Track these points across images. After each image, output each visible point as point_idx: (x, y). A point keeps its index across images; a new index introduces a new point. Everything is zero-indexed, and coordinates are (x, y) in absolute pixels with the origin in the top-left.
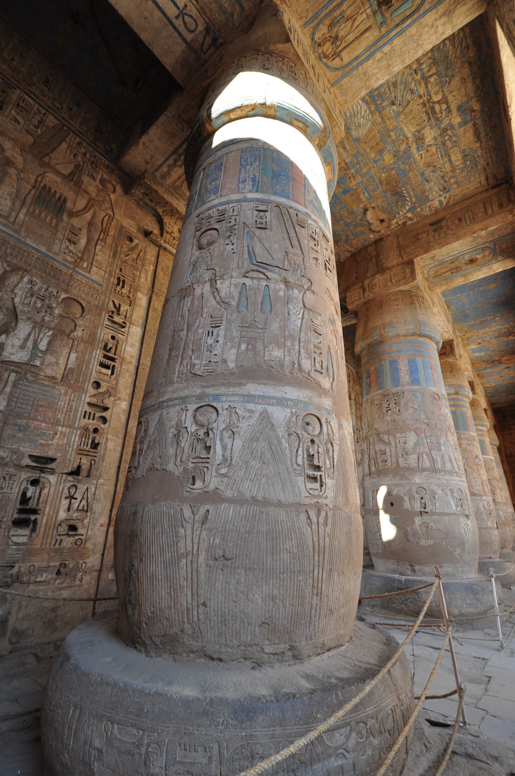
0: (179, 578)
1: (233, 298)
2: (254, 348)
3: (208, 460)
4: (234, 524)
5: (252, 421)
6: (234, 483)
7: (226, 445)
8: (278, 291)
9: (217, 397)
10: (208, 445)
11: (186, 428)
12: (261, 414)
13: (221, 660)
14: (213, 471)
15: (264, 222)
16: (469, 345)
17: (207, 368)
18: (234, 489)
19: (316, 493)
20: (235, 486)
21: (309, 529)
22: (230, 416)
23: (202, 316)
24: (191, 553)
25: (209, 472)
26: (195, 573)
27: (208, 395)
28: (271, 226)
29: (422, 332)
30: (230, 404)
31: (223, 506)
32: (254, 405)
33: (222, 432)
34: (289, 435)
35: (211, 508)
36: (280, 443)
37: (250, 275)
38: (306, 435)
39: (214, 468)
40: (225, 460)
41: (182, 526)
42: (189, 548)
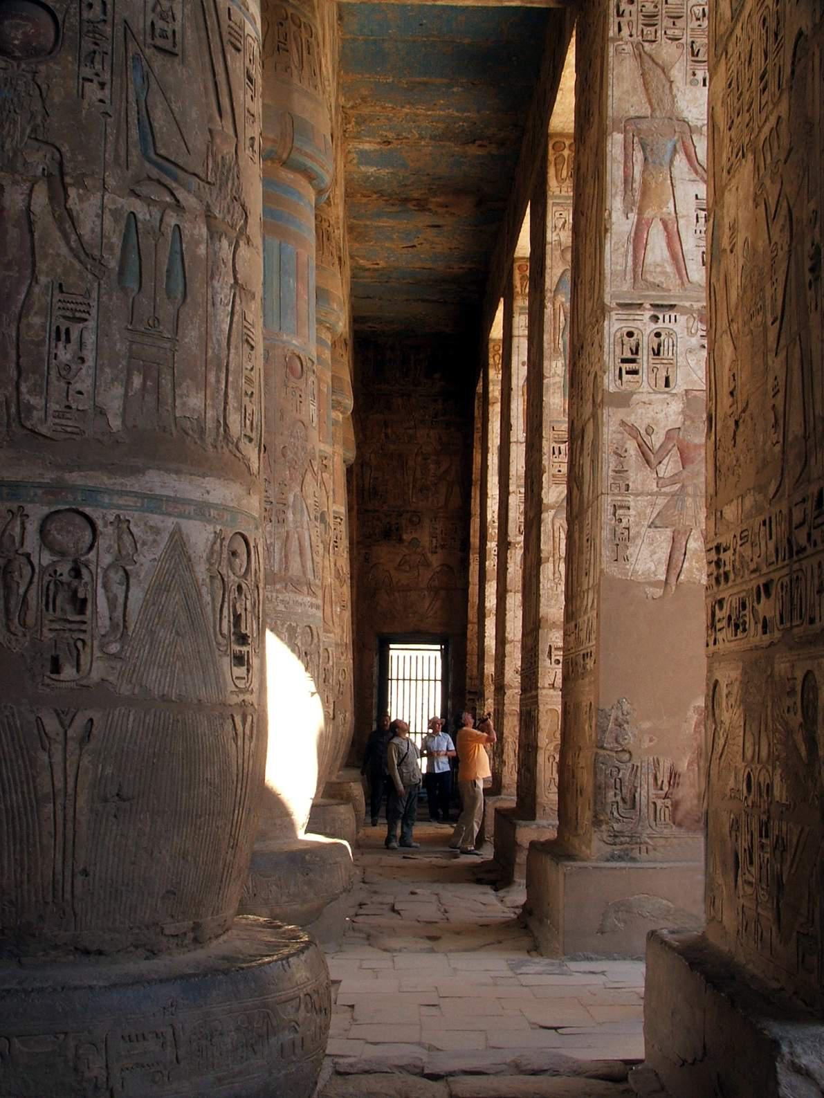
0: (40, 835)
1: (111, 248)
2: (158, 386)
3: (84, 627)
4: (135, 743)
5: (159, 551)
6: (134, 671)
7: (116, 598)
8: (197, 243)
9: (92, 494)
10: (81, 595)
11: (28, 556)
12: (172, 535)
13: (100, 953)
14: (95, 649)
15: (170, 34)
16: (358, 137)
17: (64, 422)
18: (134, 680)
19: (241, 684)
20: (135, 676)
21: (234, 746)
22: (120, 538)
23: (34, 278)
24: (62, 793)
25: (88, 650)
26: (70, 825)
27: (73, 489)
28: (183, 51)
29: (295, 155)
30: (117, 512)
31: (117, 712)
32: (161, 517)
33: (106, 571)
34: (212, 577)
35: (97, 716)
36: (199, 594)
37: (144, 190)
38: (232, 577)
39: (96, 643)
40: (114, 626)
41: (44, 749)
42: (59, 785)
